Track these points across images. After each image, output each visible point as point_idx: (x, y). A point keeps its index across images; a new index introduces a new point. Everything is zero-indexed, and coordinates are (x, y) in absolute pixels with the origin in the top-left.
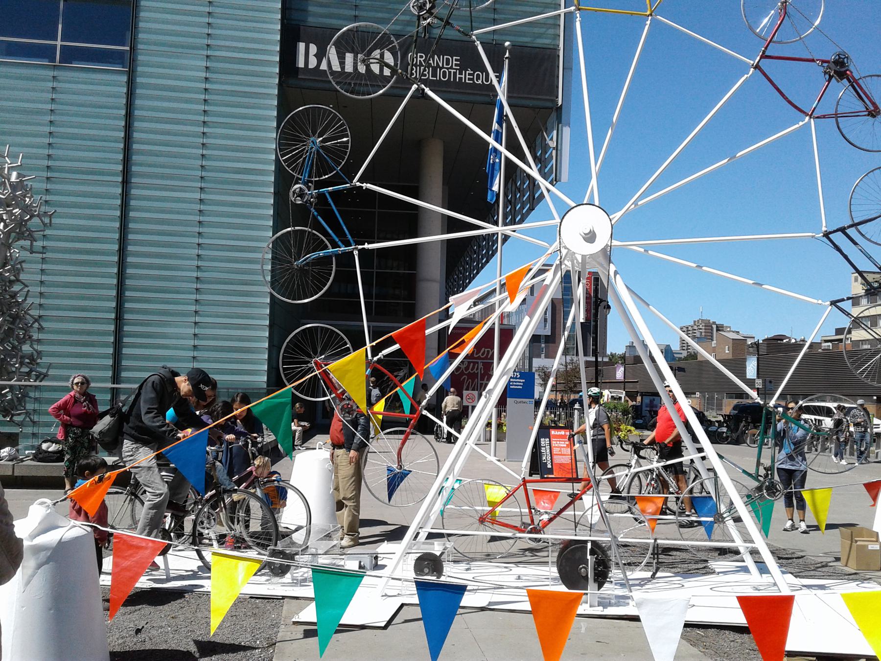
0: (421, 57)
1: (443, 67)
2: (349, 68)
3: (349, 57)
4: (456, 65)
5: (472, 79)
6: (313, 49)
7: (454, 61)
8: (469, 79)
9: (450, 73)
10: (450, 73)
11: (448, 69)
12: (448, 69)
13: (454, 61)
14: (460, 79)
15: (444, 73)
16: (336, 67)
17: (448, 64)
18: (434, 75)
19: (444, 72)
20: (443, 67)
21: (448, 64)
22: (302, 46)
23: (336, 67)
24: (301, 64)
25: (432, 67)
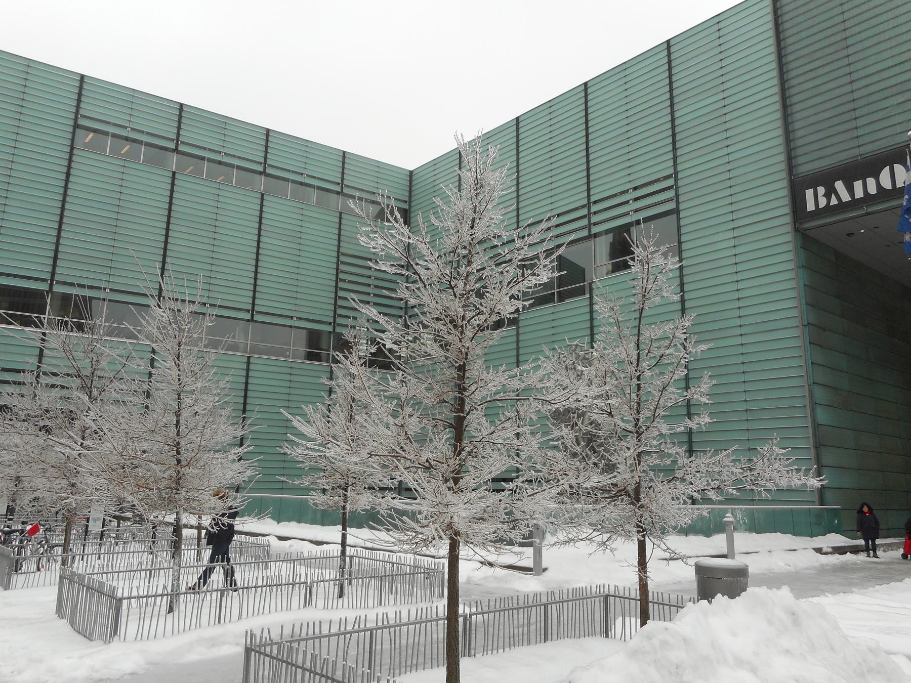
3: (858, 185)
6: (821, 190)
16: (846, 197)
22: (809, 193)
24: (811, 207)
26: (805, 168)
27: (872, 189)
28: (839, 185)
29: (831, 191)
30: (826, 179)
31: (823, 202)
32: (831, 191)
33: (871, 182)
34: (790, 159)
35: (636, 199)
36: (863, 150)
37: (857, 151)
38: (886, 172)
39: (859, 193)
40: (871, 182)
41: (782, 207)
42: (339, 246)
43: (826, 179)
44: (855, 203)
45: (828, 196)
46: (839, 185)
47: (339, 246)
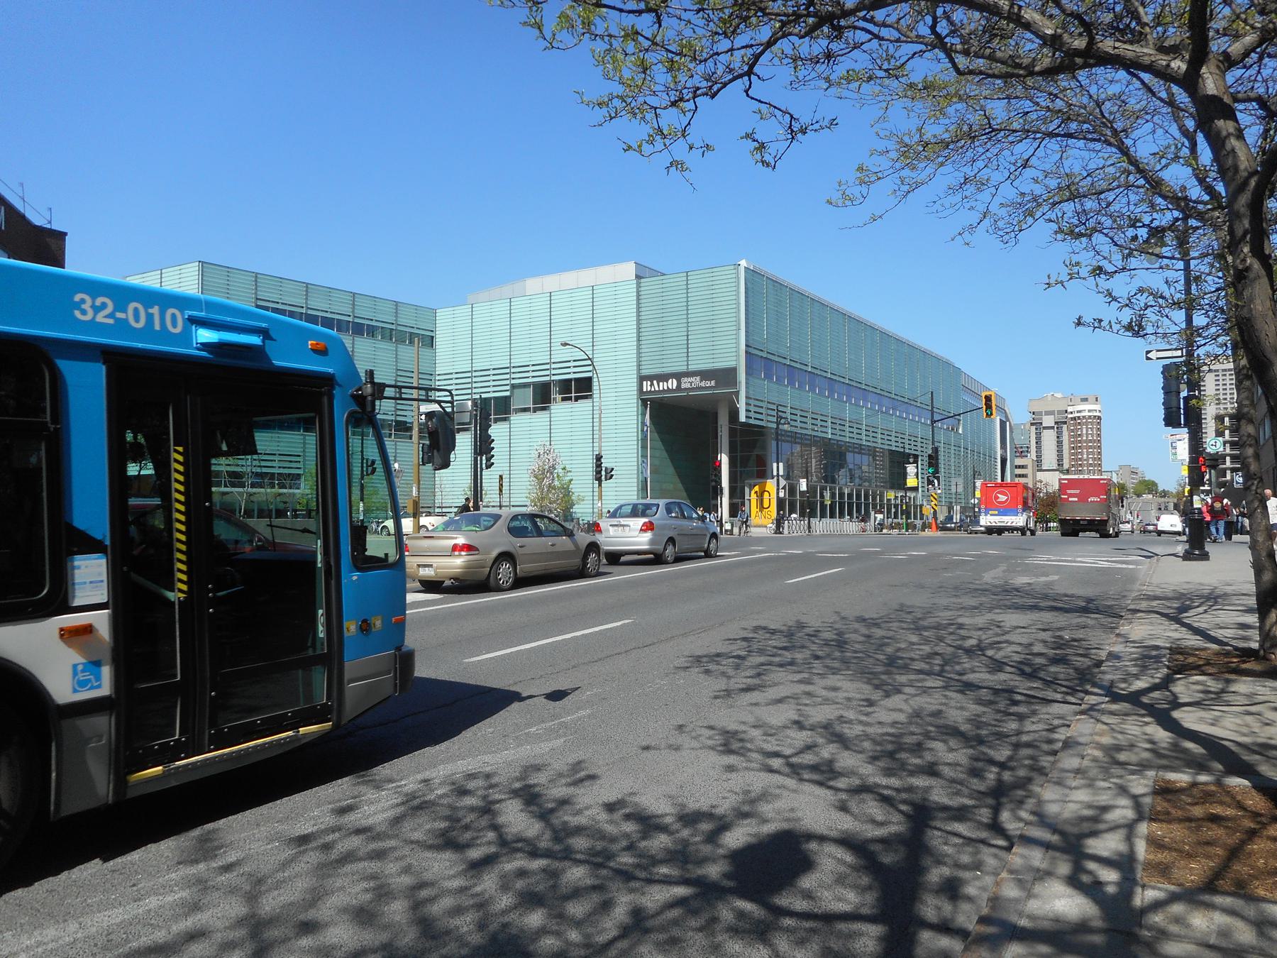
3: (661, 384)
6: (649, 383)
7: (698, 378)
13: (698, 378)
16: (657, 389)
22: (645, 383)
24: (645, 390)
26: (645, 372)
27: (666, 388)
28: (655, 382)
29: (652, 385)
30: (650, 378)
31: (649, 389)
32: (652, 385)
34: (639, 365)
35: (574, 367)
36: (663, 369)
37: (660, 370)
39: (661, 389)
40: (665, 383)
41: (635, 388)
42: (397, 366)
43: (650, 378)
44: (659, 391)
45: (651, 386)
46: (655, 382)
47: (397, 366)
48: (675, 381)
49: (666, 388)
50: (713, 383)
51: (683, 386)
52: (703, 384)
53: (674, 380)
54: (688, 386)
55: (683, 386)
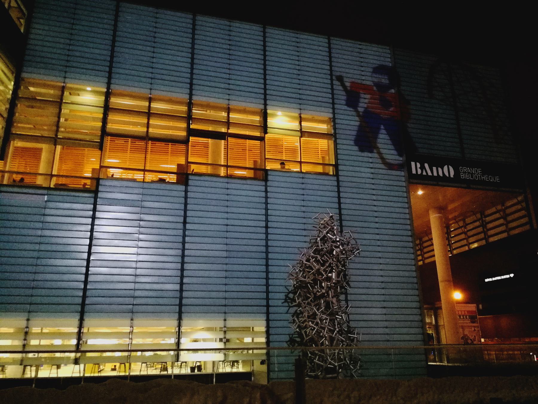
0: (465, 169)
1: (475, 174)
2: (435, 174)
4: (480, 172)
5: (488, 179)
6: (419, 165)
8: (487, 179)
9: (478, 176)
10: (478, 176)
11: (477, 174)
12: (477, 174)
14: (483, 179)
15: (476, 176)
16: (430, 173)
17: (477, 172)
18: (472, 177)
19: (476, 176)
20: (475, 174)
21: (477, 172)
22: (413, 164)
23: (430, 173)
24: (414, 172)
25: (471, 173)
27: (441, 174)
28: (426, 165)
29: (423, 168)
32: (423, 168)
33: (440, 169)
38: (446, 168)
40: (440, 170)
46: (426, 165)
48: (451, 169)
49: (441, 174)
50: (497, 179)
51: (463, 176)
52: (485, 178)
53: (450, 167)
54: (467, 177)
55: (463, 176)
